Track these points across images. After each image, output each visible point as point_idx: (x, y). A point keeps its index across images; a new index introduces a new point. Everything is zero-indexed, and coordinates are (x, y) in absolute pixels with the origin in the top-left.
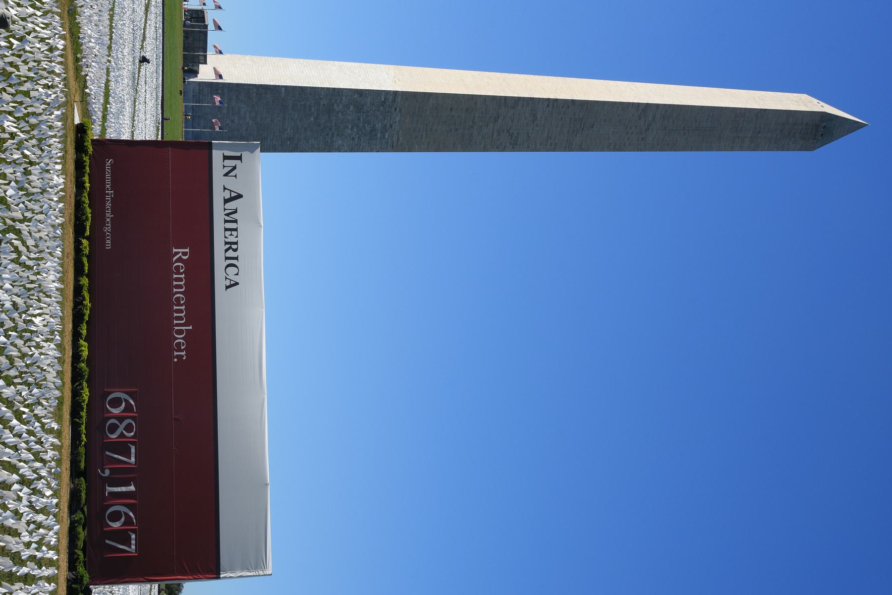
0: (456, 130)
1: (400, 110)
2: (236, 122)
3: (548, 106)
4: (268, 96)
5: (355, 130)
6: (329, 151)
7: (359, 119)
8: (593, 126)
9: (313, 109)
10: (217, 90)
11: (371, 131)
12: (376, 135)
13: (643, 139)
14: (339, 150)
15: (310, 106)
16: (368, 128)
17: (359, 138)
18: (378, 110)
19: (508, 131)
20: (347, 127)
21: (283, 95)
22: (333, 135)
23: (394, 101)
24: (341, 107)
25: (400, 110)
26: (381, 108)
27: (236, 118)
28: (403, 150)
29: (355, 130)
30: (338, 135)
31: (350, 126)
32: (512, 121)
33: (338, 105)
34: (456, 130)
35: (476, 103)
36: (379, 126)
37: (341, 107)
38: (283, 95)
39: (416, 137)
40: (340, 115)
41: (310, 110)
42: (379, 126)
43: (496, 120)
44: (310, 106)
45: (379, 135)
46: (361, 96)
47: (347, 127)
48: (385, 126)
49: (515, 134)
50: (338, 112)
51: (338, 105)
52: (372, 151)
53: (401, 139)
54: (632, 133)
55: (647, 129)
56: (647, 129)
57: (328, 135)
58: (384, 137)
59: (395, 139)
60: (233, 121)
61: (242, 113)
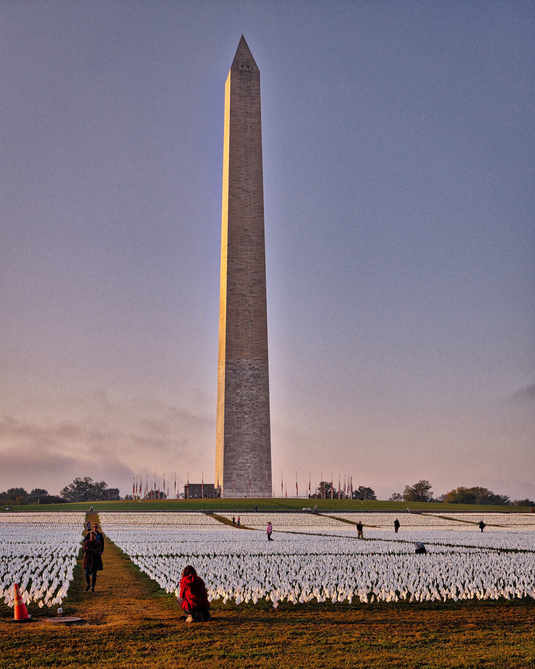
0: (251, 321)
1: (239, 359)
2: (250, 465)
3: (233, 261)
4: (232, 445)
5: (253, 388)
7: (246, 386)
8: (246, 229)
9: (240, 416)
10: (228, 477)
11: (254, 378)
12: (256, 374)
13: (254, 194)
16: (252, 380)
17: (259, 385)
19: (251, 287)
21: (231, 435)
22: (257, 402)
24: (238, 398)
25: (239, 359)
26: (237, 372)
27: (247, 465)
29: (253, 388)
30: (257, 399)
31: (251, 392)
32: (244, 284)
33: (237, 400)
34: (251, 321)
36: (250, 373)
37: (238, 398)
38: (231, 435)
39: (257, 347)
41: (240, 418)
42: (250, 373)
43: (244, 295)
45: (256, 372)
48: (250, 369)
49: (254, 282)
51: (237, 400)
52: (268, 376)
53: (259, 358)
54: (250, 202)
55: (247, 192)
56: (247, 192)
57: (257, 406)
59: (259, 362)
60: (250, 467)
61: (244, 461)
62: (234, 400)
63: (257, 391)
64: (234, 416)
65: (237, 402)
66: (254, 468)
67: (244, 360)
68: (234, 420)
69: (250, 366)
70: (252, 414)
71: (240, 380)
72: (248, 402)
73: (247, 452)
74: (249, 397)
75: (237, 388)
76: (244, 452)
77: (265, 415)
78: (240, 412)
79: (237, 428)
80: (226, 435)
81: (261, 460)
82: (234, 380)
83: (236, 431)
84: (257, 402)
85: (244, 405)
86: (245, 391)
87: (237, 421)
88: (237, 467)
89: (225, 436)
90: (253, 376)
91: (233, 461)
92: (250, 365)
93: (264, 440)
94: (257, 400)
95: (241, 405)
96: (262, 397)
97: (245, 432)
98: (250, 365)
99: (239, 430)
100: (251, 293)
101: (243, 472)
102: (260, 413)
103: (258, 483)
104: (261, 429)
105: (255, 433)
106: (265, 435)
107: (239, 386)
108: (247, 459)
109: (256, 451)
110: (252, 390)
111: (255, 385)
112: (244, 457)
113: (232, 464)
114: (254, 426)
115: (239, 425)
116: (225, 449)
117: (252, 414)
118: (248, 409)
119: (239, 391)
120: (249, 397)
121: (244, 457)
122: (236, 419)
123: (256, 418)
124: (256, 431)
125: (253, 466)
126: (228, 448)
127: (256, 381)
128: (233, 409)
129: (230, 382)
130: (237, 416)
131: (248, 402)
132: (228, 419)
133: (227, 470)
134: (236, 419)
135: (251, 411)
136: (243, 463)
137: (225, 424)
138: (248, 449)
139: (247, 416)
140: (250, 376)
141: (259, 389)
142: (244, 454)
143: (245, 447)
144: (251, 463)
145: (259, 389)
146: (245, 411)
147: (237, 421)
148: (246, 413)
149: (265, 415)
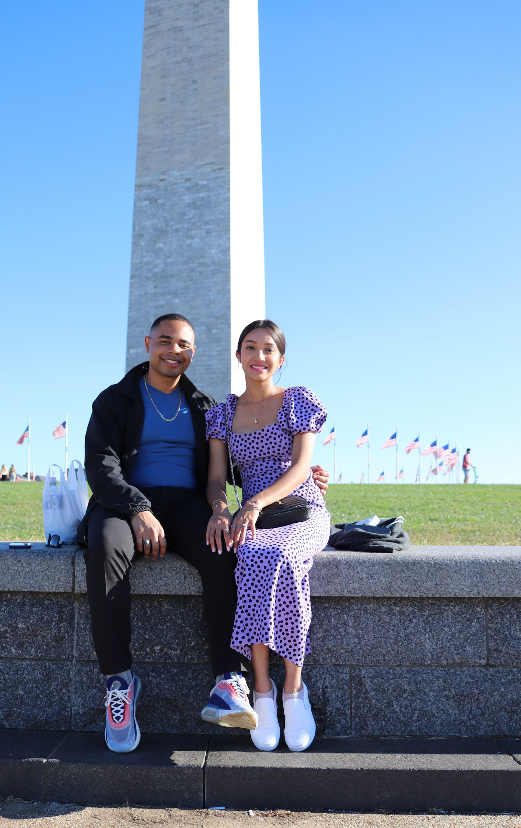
0: (194, 82)
1: (164, 173)
5: (193, 232)
6: (227, 265)
7: (177, 231)
9: (161, 302)
12: (202, 199)
14: (226, 251)
15: (157, 307)
16: (192, 213)
17: (207, 223)
18: (163, 205)
20: (190, 246)
22: (201, 265)
23: (149, 186)
24: (158, 261)
25: (164, 173)
26: (160, 201)
28: (227, 152)
29: (193, 232)
30: (202, 257)
31: (188, 242)
33: (156, 266)
34: (194, 82)
35: (153, 68)
40: (170, 260)
42: (188, 198)
43: (179, 30)
44: (157, 307)
45: (202, 195)
46: (141, 236)
47: (190, 246)
48: (188, 189)
50: (166, 264)
51: (156, 266)
52: (228, 200)
53: (209, 160)
57: (201, 273)
58: (204, 186)
59: (208, 169)
67: (177, 173)
69: (188, 184)
72: (181, 267)
78: (163, 294)
80: (131, 351)
82: (152, 222)
84: (201, 265)
85: (172, 276)
89: (128, 352)
90: (194, 205)
92: (187, 180)
94: (202, 260)
98: (187, 180)
100: (196, 20)
106: (218, 340)
107: (161, 233)
110: (192, 237)
119: (161, 245)
131: (181, 267)
135: (186, 288)
137: (130, 325)
139: (177, 301)
140: (189, 205)
141: (208, 232)
148: (175, 294)
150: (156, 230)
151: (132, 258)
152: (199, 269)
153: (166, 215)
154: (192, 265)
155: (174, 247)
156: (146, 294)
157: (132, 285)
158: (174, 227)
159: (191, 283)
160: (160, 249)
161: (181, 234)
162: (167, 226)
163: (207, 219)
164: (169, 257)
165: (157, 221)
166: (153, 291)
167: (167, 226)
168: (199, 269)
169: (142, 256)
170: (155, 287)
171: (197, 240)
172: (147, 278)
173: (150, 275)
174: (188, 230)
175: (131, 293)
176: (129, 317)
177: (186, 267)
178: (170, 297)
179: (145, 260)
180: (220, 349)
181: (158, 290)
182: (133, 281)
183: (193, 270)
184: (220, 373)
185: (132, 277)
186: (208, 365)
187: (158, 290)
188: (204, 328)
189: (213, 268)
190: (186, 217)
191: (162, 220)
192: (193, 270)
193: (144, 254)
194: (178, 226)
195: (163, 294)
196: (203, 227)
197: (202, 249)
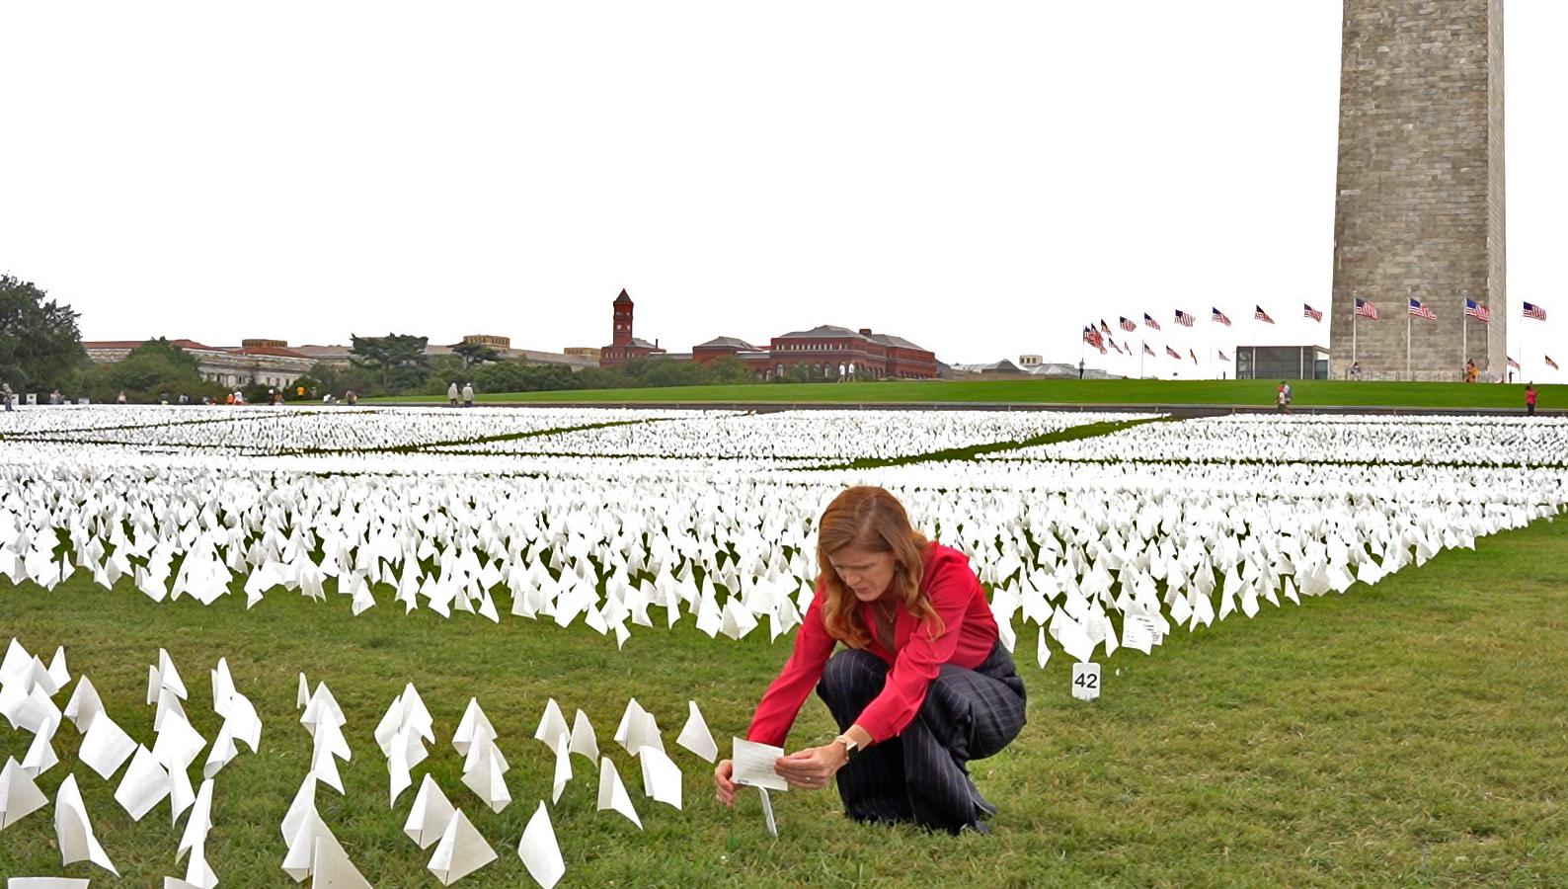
2: (1417, 281)
4: (1359, 221)
5: (1433, 33)
7: (1408, 30)
9: (1387, 128)
15: (1379, 134)
17: (1453, 21)
20: (1428, 52)
21: (1357, 192)
22: (1444, 79)
24: (1382, 71)
27: (1407, 282)
29: (1433, 33)
30: (1446, 68)
31: (1425, 46)
38: (1357, 192)
40: (1399, 70)
41: (1389, 133)
44: (1379, 134)
46: (1356, 34)
47: (1428, 52)
50: (1393, 75)
51: (1378, 77)
57: (1445, 90)
61: (1397, 270)
62: (1370, 78)
63: (1446, 42)
64: (1371, 130)
65: (1377, 83)
66: (1429, 293)
68: (1366, 141)
70: (1429, 119)
71: (1391, 14)
72: (1414, 81)
73: (1407, 243)
74: (1418, 65)
75: (1381, 40)
76: (1398, 241)
77: (1470, 118)
78: (1388, 117)
79: (1378, 166)
80: (1342, 192)
81: (1453, 266)
82: (1371, 16)
83: (1374, 176)
84: (1444, 79)
85: (1402, 92)
86: (1406, 48)
87: (1378, 146)
88: (1375, 289)
91: (1361, 272)
93: (1466, 199)
94: (1446, 73)
95: (1391, 93)
96: (1463, 61)
97: (1403, 178)
99: (1385, 174)
101: (1393, 306)
102: (1455, 113)
103: (1440, 339)
104: (1456, 167)
105: (1434, 177)
107: (1385, 32)
108: (1408, 265)
109: (1438, 236)
110: (1431, 40)
111: (1440, 22)
112: (1399, 259)
113: (1360, 283)
114: (1431, 158)
115: (1383, 157)
116: (1336, 237)
117: (1429, 119)
118: (1414, 104)
119: (1386, 49)
120: (1418, 65)
121: (1399, 259)
122: (1377, 139)
123: (1442, 129)
124: (1438, 172)
125: (1425, 285)
126: (1347, 232)
127: (1444, 10)
128: (1366, 107)
129: (1357, 24)
130: (1379, 129)
131: (1414, 81)
132: (1347, 141)
133: (1342, 300)
134: (1377, 139)
135: (1423, 110)
136: (1396, 277)
138: (1412, 230)
139: (1411, 126)
141: (1455, 34)
142: (1399, 247)
143: (1403, 225)
144: (1421, 276)
145: (1455, 34)
146: (1403, 110)
147: (1378, 146)
148: (1407, 118)
149: (1470, 118)
150: (1378, 26)
151: (1343, 66)
152: (1442, 85)
153: (1392, 7)
154: (1431, 79)
155: (1404, 53)
156: (1364, 115)
157: (1342, 102)
158: (1405, 25)
159: (1429, 103)
160: (1385, 54)
161: (1414, 35)
162: (1394, 22)
163: (1453, 16)
164: (1398, 66)
165: (1379, 15)
166: (1375, 111)
167: (1394, 22)
168: (1442, 85)
169: (1358, 63)
170: (1377, 107)
171: (1438, 44)
172: (1365, 94)
173: (1370, 89)
174: (1425, 31)
175: (1341, 112)
176: (1340, 147)
177: (1422, 80)
178: (1399, 121)
179: (1361, 68)
180: (1473, 193)
181: (1380, 111)
182: (1345, 95)
183: (1433, 86)
184: (1474, 226)
185: (1343, 91)
186: (1457, 215)
187: (1380, 111)
188: (1449, 166)
189: (1462, 84)
190: (1421, 12)
191: (1386, 14)
192: (1433, 86)
193: (1360, 60)
194: (1410, 24)
195: (1388, 117)
196: (1447, 27)
197: (1446, 58)
